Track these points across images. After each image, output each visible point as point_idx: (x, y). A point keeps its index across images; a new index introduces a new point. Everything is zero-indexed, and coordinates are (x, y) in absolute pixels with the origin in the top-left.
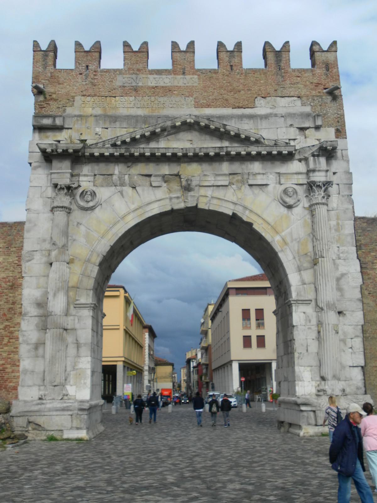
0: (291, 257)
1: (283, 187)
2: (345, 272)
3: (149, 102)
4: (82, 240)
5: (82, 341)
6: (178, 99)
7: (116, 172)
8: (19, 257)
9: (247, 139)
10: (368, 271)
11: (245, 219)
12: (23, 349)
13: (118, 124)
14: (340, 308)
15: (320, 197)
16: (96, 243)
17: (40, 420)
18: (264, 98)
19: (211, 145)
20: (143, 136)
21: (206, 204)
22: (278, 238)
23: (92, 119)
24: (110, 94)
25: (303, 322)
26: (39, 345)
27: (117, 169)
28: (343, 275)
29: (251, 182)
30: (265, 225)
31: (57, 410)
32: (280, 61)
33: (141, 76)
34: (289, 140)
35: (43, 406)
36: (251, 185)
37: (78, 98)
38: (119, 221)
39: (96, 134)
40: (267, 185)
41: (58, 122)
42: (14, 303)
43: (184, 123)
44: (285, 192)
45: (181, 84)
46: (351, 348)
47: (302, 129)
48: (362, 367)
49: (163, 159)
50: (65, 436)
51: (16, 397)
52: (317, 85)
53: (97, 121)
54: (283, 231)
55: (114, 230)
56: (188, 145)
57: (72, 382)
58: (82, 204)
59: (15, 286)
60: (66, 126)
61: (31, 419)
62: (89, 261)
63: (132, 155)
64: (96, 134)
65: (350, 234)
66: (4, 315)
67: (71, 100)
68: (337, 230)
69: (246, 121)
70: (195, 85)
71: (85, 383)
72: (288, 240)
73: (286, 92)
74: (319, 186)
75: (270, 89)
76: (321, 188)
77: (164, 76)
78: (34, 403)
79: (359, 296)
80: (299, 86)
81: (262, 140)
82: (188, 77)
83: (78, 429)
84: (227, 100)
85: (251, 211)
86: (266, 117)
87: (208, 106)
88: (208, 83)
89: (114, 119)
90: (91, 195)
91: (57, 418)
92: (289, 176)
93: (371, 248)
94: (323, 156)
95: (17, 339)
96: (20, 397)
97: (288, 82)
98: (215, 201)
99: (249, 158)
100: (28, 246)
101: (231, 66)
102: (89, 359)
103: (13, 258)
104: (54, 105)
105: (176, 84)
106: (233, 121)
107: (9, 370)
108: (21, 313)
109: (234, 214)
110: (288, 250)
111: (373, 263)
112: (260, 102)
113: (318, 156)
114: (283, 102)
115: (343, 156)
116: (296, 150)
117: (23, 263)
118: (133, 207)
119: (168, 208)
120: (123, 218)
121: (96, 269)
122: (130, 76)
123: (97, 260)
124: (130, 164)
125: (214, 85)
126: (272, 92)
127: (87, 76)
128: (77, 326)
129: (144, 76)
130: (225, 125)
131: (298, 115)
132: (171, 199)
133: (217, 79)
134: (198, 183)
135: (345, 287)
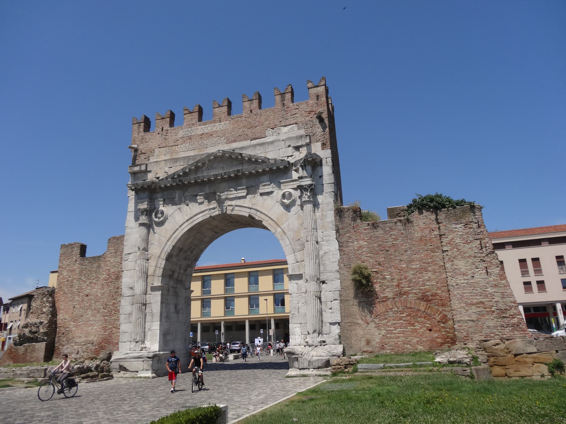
0: (288, 243)
1: (282, 192)
2: (327, 250)
3: (198, 145)
4: (157, 243)
5: (154, 311)
6: (215, 140)
7: (177, 196)
8: (121, 258)
9: (256, 161)
10: (344, 249)
11: (257, 218)
12: (122, 318)
13: (178, 163)
14: (322, 278)
15: (306, 197)
16: (164, 245)
17: (126, 365)
18: (273, 129)
19: (232, 170)
20: (190, 170)
21: (232, 211)
22: (279, 230)
23: (163, 163)
24: (175, 144)
25: (296, 291)
26: (130, 314)
27: (177, 194)
28: (325, 253)
29: (261, 191)
30: (270, 221)
31: (135, 358)
32: (284, 100)
33: (194, 128)
34: (288, 157)
35: (127, 355)
36: (262, 194)
37: (157, 151)
38: (178, 229)
39: (165, 172)
40: (272, 192)
41: (143, 168)
42: (118, 288)
43: (216, 157)
44: (284, 196)
45: (218, 129)
46: (331, 309)
47: (297, 148)
48: (339, 323)
49: (203, 183)
50: (139, 375)
51: (118, 350)
52: (310, 112)
53: (166, 163)
54: (283, 224)
55: (175, 235)
56: (221, 171)
57: (148, 339)
58: (156, 220)
59: (118, 277)
60: (148, 170)
61: (122, 364)
62: (159, 257)
63: (183, 184)
64: (165, 172)
65: (331, 221)
66: (113, 296)
67: (152, 151)
68: (321, 219)
69: (258, 147)
70: (227, 127)
71: (156, 340)
72: (286, 231)
73: (288, 122)
74: (306, 190)
75: (277, 123)
76: (308, 190)
77: (207, 126)
78: (126, 352)
79: (338, 268)
80: (297, 115)
81: (267, 160)
82: (223, 123)
83: (147, 370)
84: (247, 135)
85: (261, 212)
86: (272, 142)
87: (235, 141)
88: (236, 125)
89: (176, 160)
90: (161, 213)
91: (135, 363)
92: (287, 184)
93: (346, 230)
94: (308, 164)
95: (119, 311)
96: (120, 349)
97: (289, 114)
98: (236, 208)
99: (258, 174)
100: (126, 252)
101: (251, 111)
102: (159, 323)
103: (118, 260)
104: (143, 156)
105: (215, 129)
106: (250, 148)
107: (114, 332)
108: (121, 295)
109: (249, 215)
110: (286, 238)
111: (347, 242)
112: (270, 131)
113: (305, 166)
114: (285, 129)
115: (327, 163)
116: (292, 164)
117: (123, 263)
118: (187, 218)
119: (208, 216)
120: (180, 227)
121: (164, 262)
122: (186, 130)
123: (164, 256)
124: (184, 189)
125: (239, 126)
126: (278, 123)
127: (162, 135)
128: (152, 301)
129: (195, 128)
130: (241, 154)
131: (294, 137)
132: (210, 209)
133: (241, 121)
134: (226, 196)
135: (327, 262)
